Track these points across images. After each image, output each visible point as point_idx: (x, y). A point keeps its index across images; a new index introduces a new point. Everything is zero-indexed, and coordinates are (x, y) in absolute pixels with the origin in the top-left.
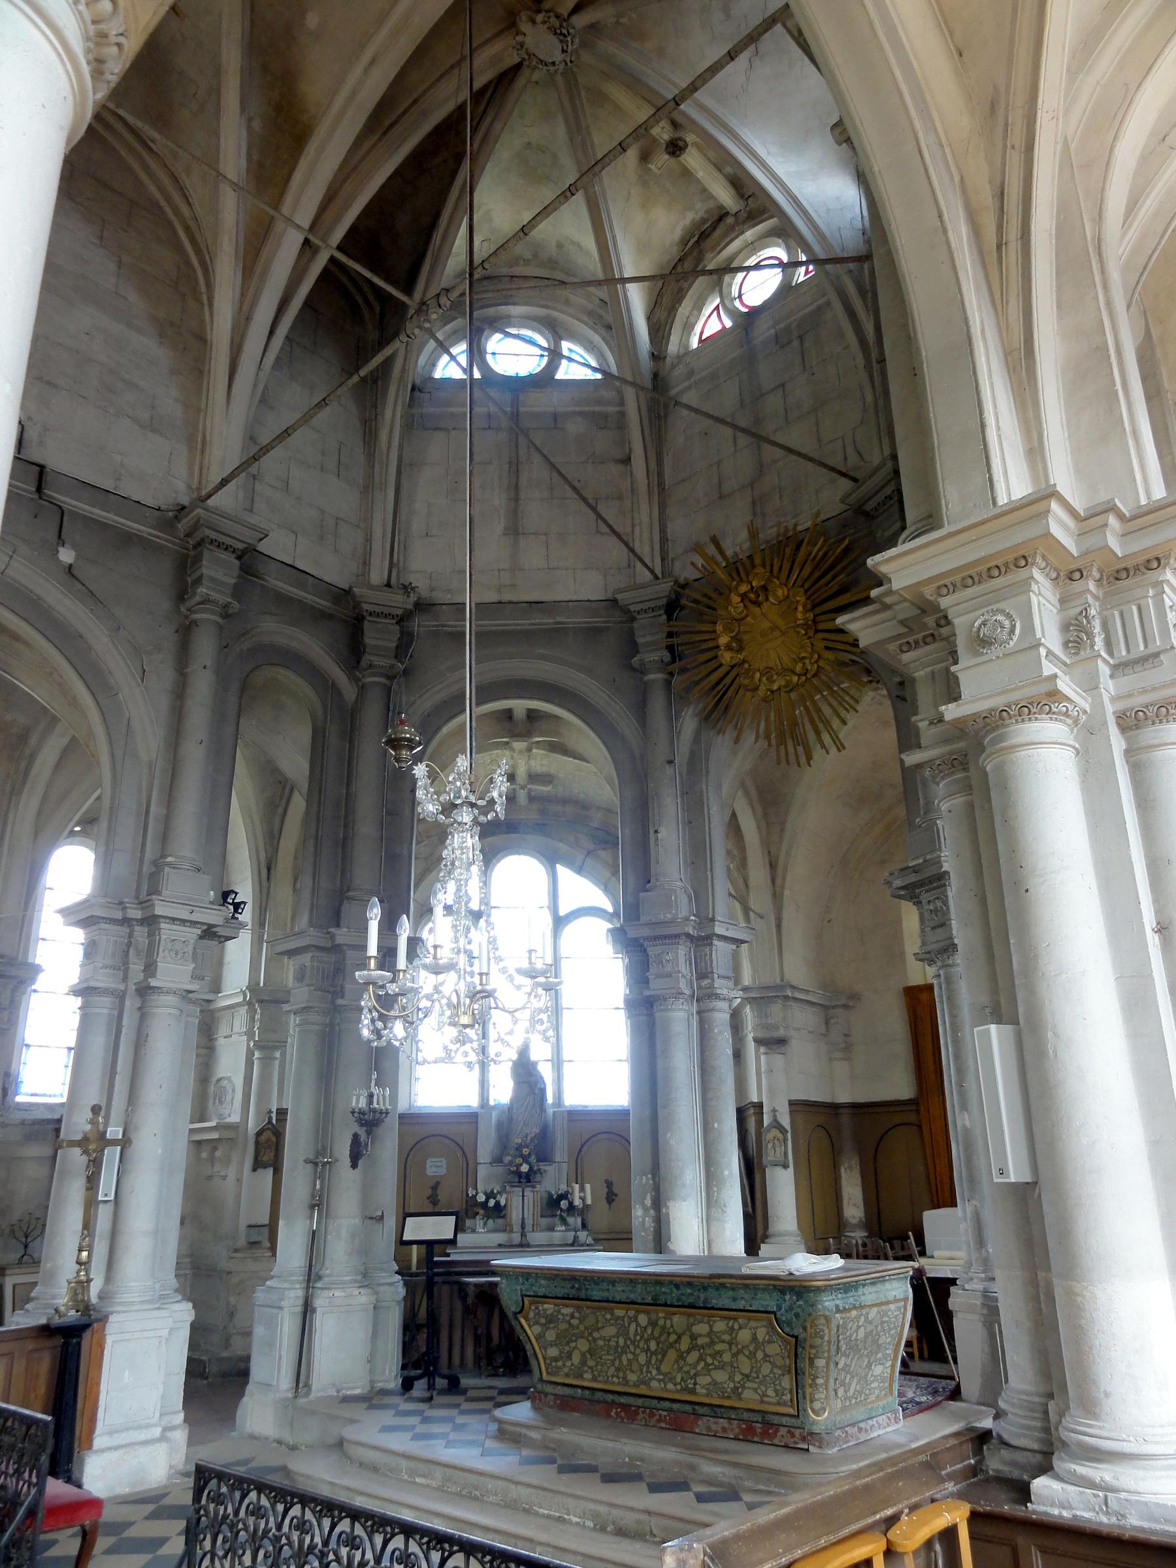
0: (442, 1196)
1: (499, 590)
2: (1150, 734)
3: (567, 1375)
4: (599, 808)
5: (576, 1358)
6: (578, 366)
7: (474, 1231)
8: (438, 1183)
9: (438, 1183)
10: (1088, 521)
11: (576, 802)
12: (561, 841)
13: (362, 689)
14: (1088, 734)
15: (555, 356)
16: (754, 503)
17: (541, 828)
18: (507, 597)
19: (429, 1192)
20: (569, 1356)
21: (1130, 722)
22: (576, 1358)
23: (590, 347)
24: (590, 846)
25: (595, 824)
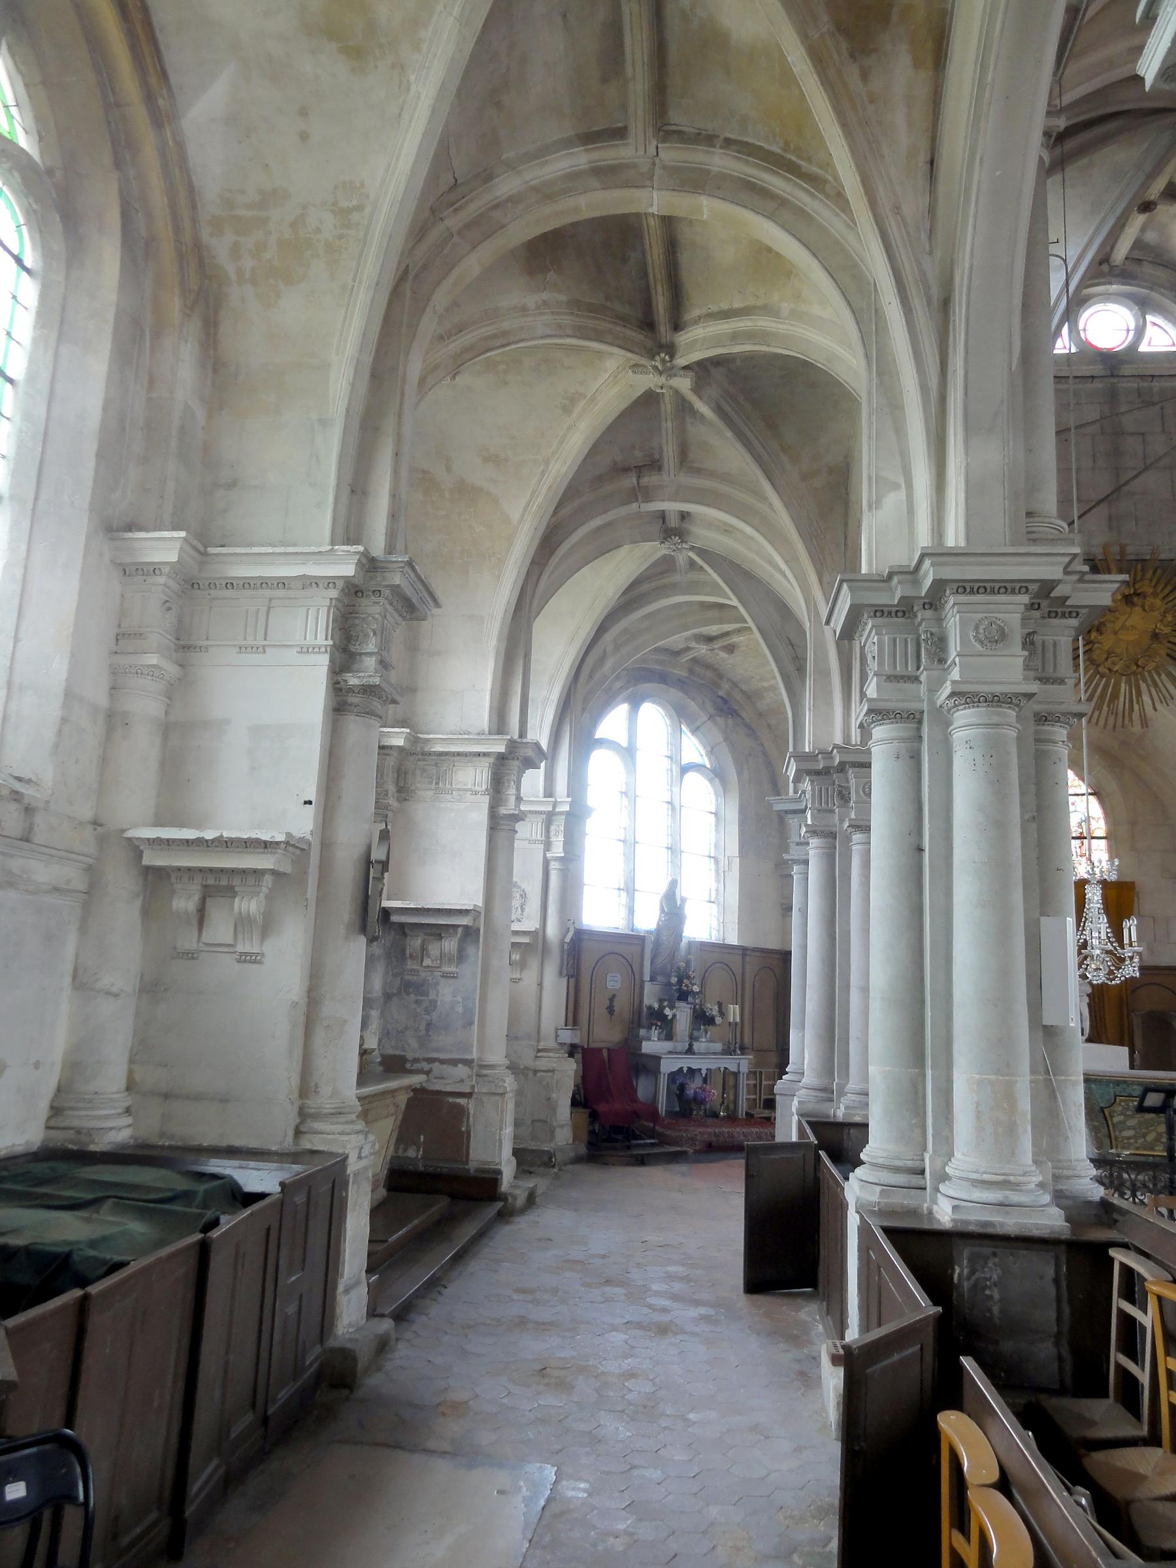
0: (617, 1004)
3: (1137, 1149)
4: (729, 680)
5: (1151, 1137)
7: (649, 1039)
8: (614, 996)
9: (614, 996)
11: (715, 670)
12: (693, 699)
16: (1110, 518)
17: (681, 684)
19: (607, 1003)
20: (1144, 1136)
22: (1151, 1137)
24: (712, 711)
25: (721, 693)
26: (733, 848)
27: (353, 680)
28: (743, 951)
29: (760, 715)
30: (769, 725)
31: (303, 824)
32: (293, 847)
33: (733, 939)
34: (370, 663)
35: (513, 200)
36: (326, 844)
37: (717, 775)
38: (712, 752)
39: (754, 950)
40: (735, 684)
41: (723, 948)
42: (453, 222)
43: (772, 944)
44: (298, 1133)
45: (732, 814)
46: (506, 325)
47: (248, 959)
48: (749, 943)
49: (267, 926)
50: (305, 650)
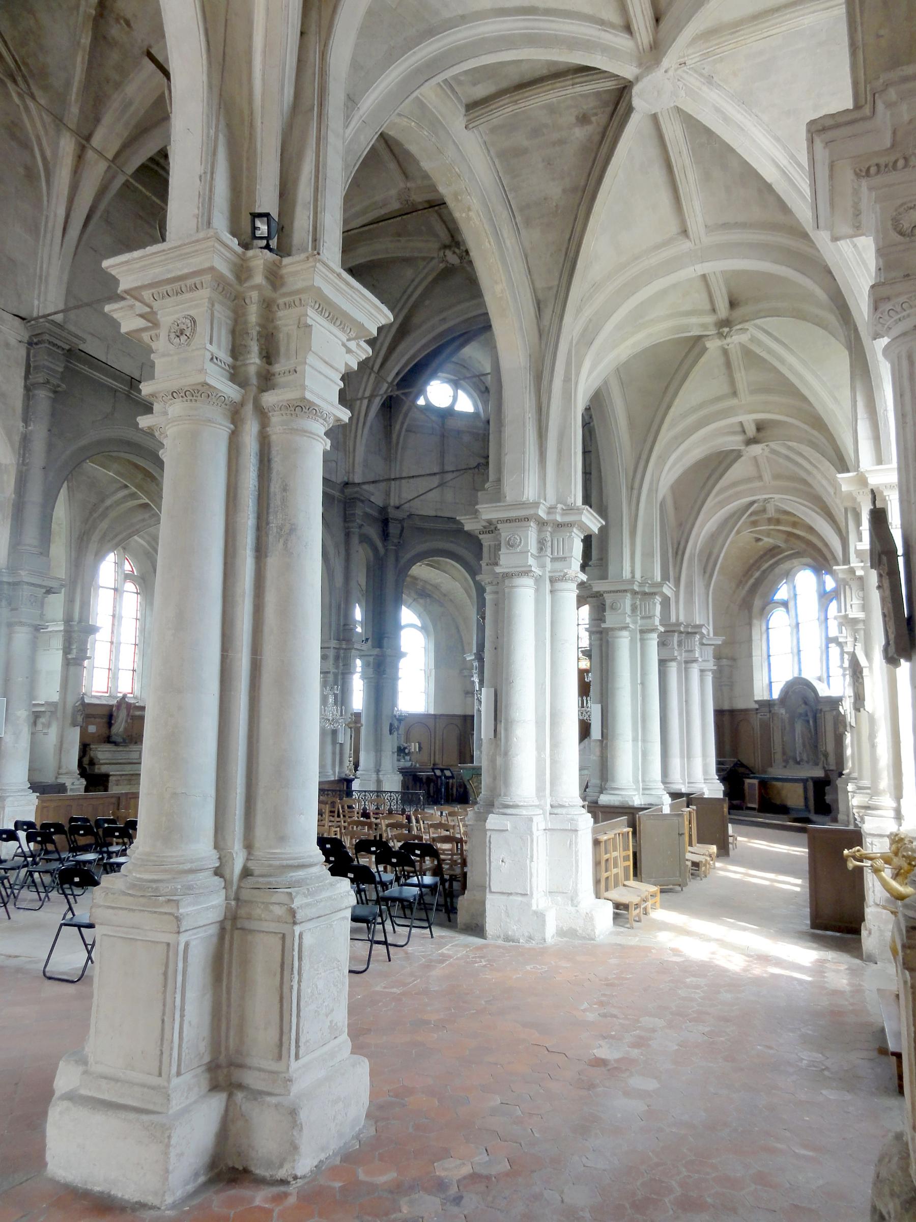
1: (436, 510)
2: (689, 665)
6: (465, 404)
10: (687, 626)
13: (387, 550)
14: (679, 664)
15: (455, 398)
18: (439, 514)
21: (686, 662)
23: (470, 396)
26: (432, 665)
27: (69, 656)
28: (435, 716)
29: (445, 595)
30: (451, 600)
31: (55, 697)
32: (54, 705)
33: (432, 712)
34: (75, 651)
35: (111, 506)
36: (65, 703)
37: (424, 629)
38: (420, 617)
39: (441, 715)
40: (425, 582)
41: (427, 716)
42: (95, 515)
43: (459, 711)
44: (57, 778)
45: (432, 647)
46: (138, 527)
47: (46, 734)
48: (436, 713)
49: (49, 725)
50: (57, 649)
